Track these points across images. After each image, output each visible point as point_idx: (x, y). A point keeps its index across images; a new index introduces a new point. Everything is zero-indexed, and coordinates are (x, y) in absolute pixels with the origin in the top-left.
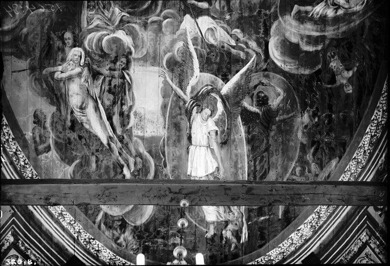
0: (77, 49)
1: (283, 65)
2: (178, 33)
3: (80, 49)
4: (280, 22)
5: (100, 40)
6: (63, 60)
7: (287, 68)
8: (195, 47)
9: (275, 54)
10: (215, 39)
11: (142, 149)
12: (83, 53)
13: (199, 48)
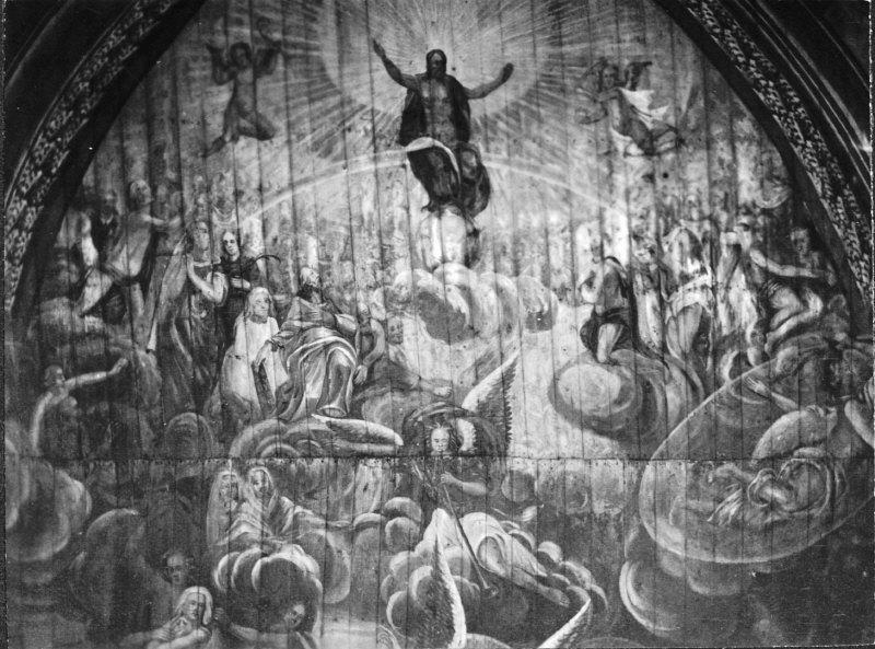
0: (194, 590)
1: (651, 625)
2: (420, 547)
3: (203, 591)
4: (642, 529)
5: (246, 568)
6: (171, 614)
7: (661, 629)
8: (458, 577)
9: (630, 596)
10: (501, 561)
12: (209, 599)
13: (466, 581)
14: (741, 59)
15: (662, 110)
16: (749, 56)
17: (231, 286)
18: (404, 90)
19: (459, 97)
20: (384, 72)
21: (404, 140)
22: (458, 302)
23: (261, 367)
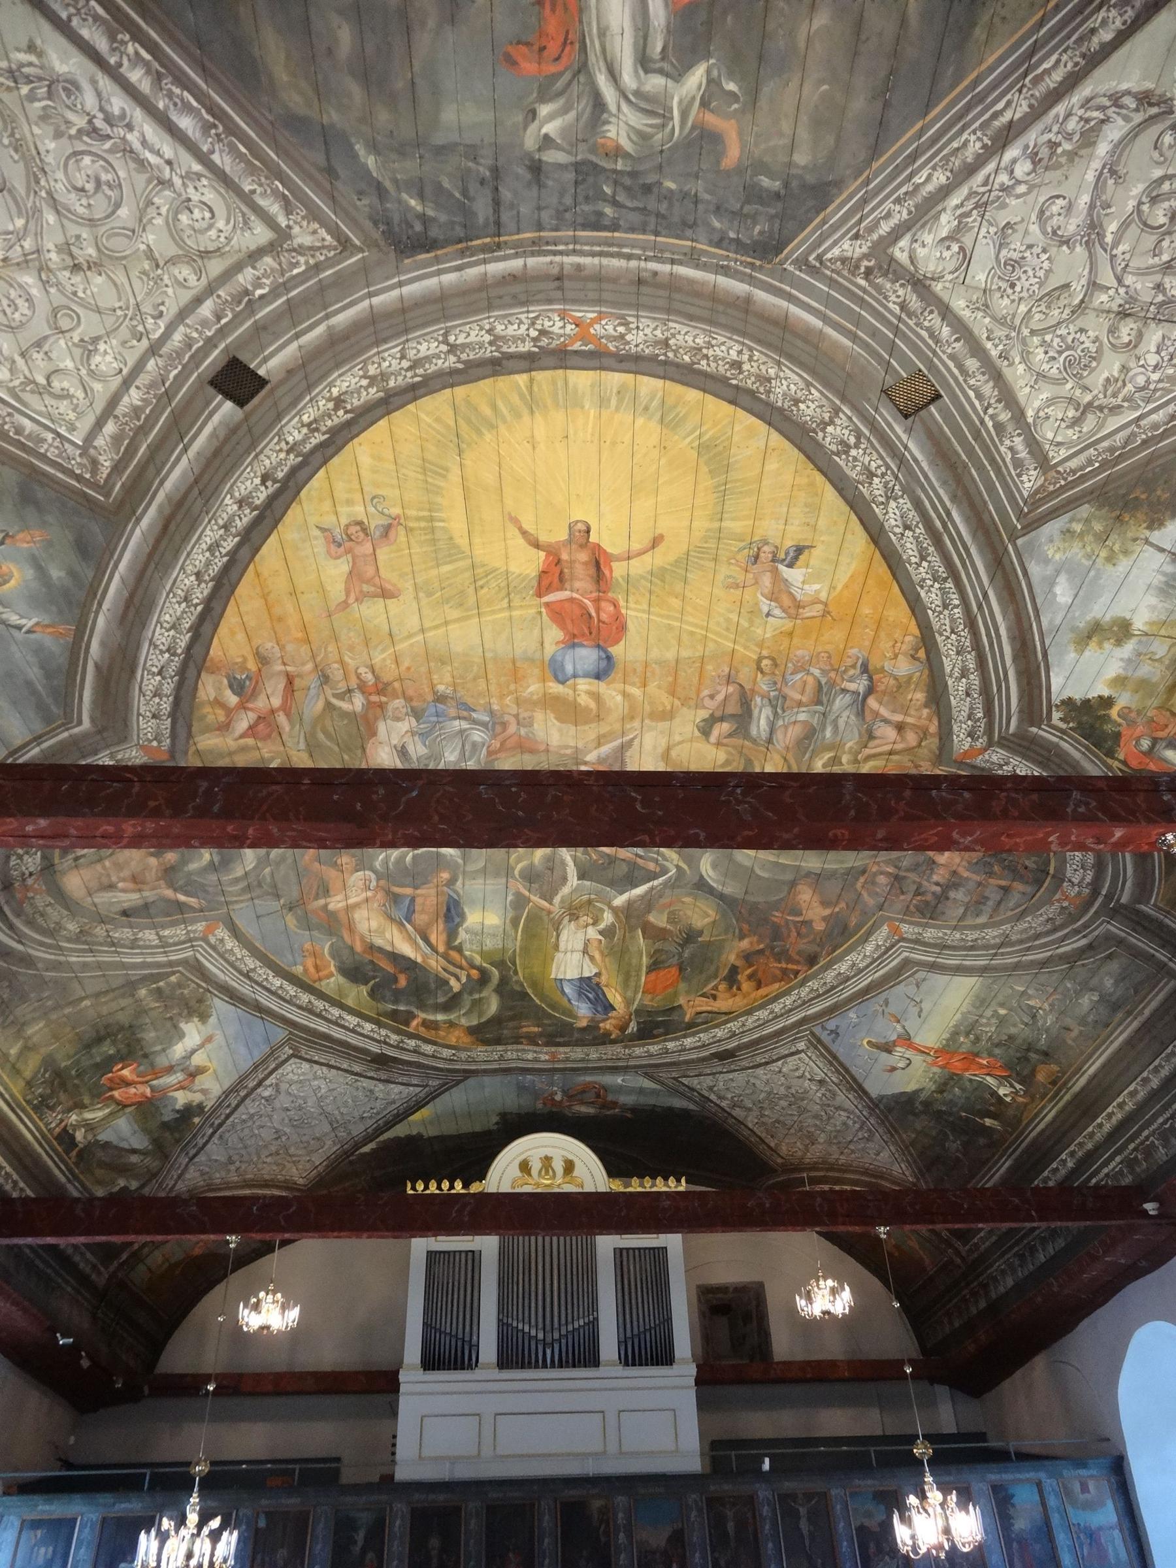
7: (728, 890)
11: (478, 960)
12: (373, 876)
14: (913, 560)
15: (817, 587)
16: (923, 558)
17: (369, 702)
18: (542, 554)
19: (599, 563)
20: (521, 541)
21: (539, 595)
22: (584, 700)
23: (403, 747)
